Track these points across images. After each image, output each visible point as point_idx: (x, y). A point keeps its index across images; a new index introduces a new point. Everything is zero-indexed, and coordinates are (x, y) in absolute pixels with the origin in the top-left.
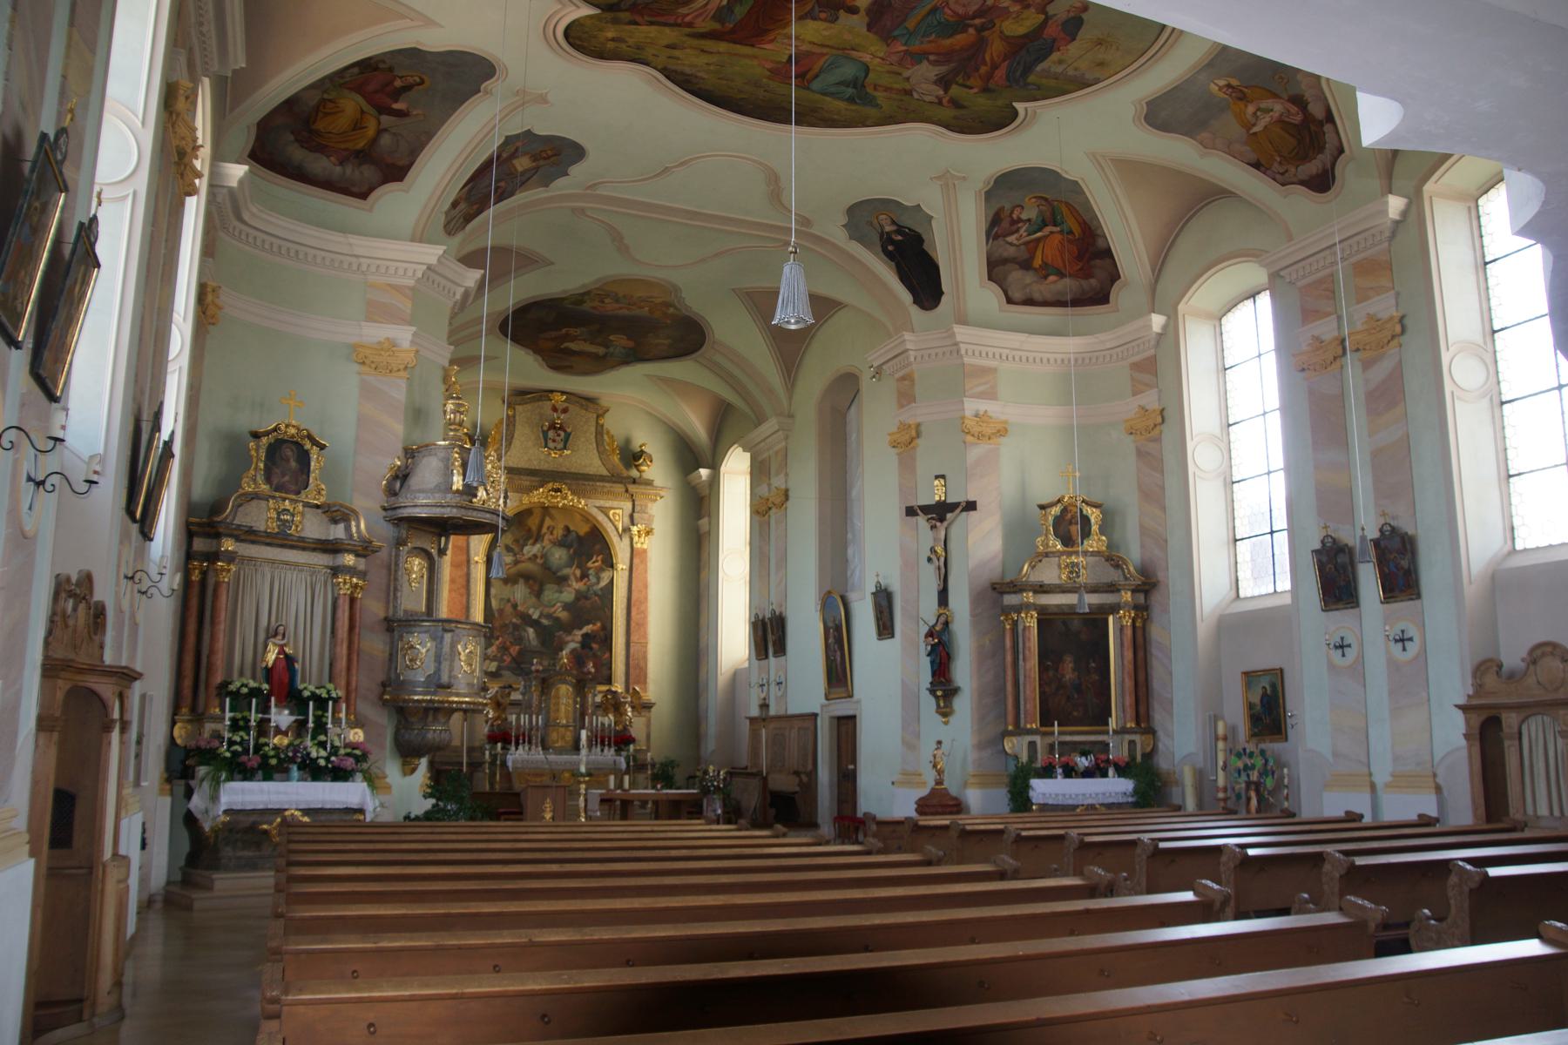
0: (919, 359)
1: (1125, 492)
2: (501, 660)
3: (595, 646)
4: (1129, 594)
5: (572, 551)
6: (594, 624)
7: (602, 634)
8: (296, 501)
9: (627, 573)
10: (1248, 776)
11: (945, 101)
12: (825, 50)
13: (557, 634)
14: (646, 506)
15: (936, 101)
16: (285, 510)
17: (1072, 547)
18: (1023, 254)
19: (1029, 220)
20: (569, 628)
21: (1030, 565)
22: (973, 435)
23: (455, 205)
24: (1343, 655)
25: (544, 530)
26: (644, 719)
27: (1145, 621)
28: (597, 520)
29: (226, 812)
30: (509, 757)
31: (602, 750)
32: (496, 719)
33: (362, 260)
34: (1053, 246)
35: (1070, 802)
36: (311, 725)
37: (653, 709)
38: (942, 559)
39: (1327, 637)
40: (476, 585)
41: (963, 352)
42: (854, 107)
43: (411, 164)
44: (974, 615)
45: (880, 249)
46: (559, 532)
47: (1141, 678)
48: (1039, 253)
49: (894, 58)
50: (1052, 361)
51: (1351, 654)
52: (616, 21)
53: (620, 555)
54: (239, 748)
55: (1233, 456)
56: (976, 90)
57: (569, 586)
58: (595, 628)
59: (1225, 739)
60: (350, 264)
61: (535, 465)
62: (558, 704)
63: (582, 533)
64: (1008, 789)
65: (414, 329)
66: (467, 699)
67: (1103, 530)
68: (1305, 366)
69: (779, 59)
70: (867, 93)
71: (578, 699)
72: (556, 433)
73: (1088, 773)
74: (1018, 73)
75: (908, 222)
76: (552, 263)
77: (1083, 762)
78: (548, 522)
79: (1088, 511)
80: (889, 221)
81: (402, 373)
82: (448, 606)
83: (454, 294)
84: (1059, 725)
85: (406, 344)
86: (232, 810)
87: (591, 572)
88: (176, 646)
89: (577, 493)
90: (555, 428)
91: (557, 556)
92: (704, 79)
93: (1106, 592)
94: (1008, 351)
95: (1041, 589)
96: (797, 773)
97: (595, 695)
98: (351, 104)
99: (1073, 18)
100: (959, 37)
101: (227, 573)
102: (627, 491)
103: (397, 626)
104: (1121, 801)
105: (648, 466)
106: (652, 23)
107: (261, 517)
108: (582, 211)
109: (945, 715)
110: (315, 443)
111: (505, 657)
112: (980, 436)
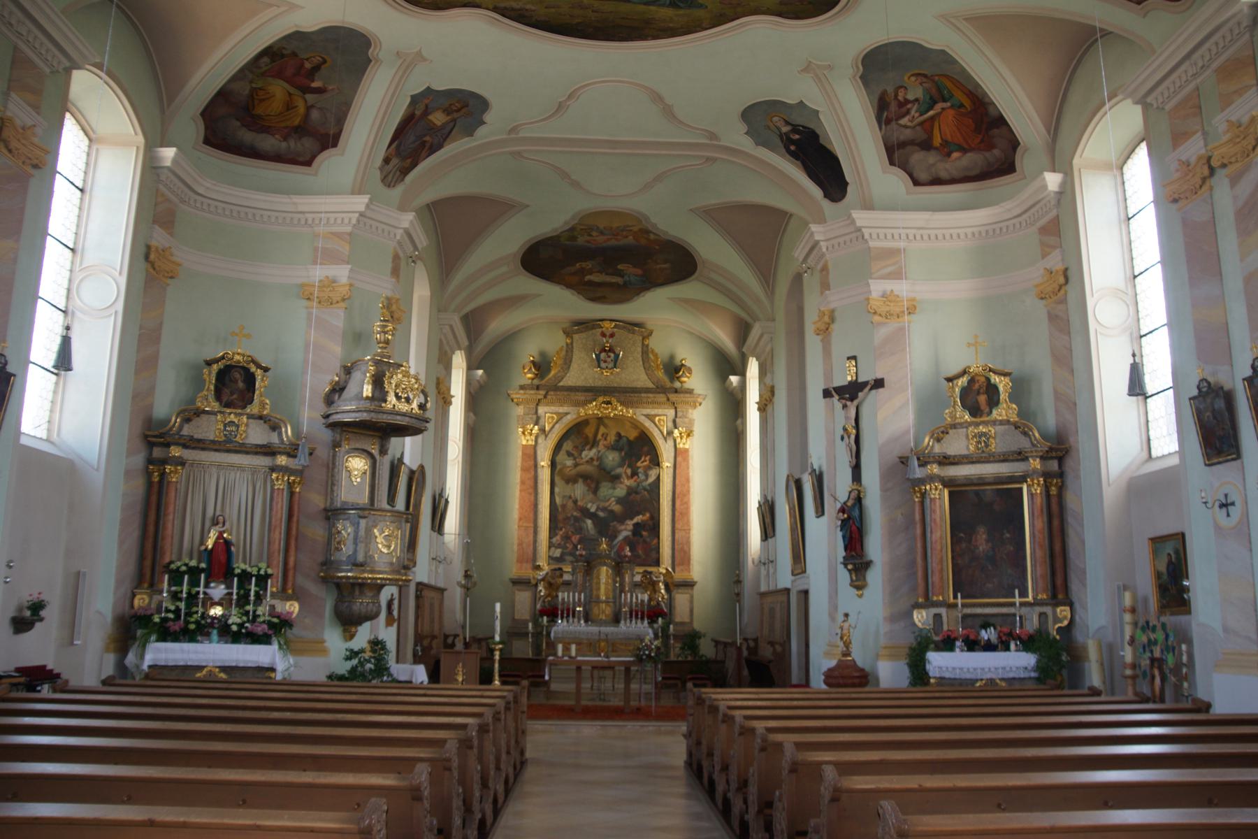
0: (830, 249)
1: (1038, 360)
2: (564, 547)
3: (644, 533)
4: (1038, 460)
5: (623, 454)
6: (644, 515)
7: (650, 523)
8: (241, 414)
9: (672, 470)
10: (1152, 652)
13: (612, 524)
14: (687, 412)
16: (230, 422)
17: (981, 416)
18: (920, 134)
19: (917, 100)
20: (622, 519)
21: (931, 437)
22: (880, 315)
23: (387, 161)
24: (1228, 515)
25: (599, 437)
26: (688, 595)
27: (1061, 488)
28: (645, 427)
29: (150, 667)
30: (554, 629)
31: (636, 623)
32: (546, 596)
33: (307, 215)
34: (948, 125)
35: (968, 676)
36: (252, 598)
37: (695, 588)
38: (853, 437)
39: (1203, 495)
40: (542, 485)
41: (867, 236)
42: (681, 12)
43: (341, 131)
44: (884, 489)
45: (784, 150)
46: (612, 438)
47: (1057, 547)
48: (936, 132)
50: (962, 236)
51: (1235, 512)
54: (171, 616)
55: (1140, 309)
57: (621, 483)
58: (645, 518)
59: (1133, 610)
60: (299, 220)
61: (590, 383)
62: (599, 583)
63: (631, 438)
64: (907, 661)
65: (350, 266)
66: (389, 577)
67: (1015, 397)
68: (1176, 196)
71: (618, 579)
72: (607, 355)
73: (989, 647)
75: (799, 120)
76: (528, 206)
77: (987, 635)
78: (602, 430)
79: (995, 379)
80: (783, 123)
81: (342, 305)
82: (520, 504)
83: (395, 235)
84: (962, 598)
85: (344, 280)
86: (156, 665)
87: (640, 470)
88: (135, 534)
89: (626, 404)
90: (605, 351)
91: (611, 458)
92: (534, 11)
93: (1018, 460)
94: (914, 231)
95: (945, 461)
96: (772, 644)
97: (633, 575)
98: (278, 89)
101: (176, 476)
102: (668, 400)
103: (332, 514)
104: (1022, 676)
105: (689, 378)
107: (209, 429)
108: (519, 153)
109: (859, 588)
110: (259, 366)
111: (568, 545)
112: (888, 315)
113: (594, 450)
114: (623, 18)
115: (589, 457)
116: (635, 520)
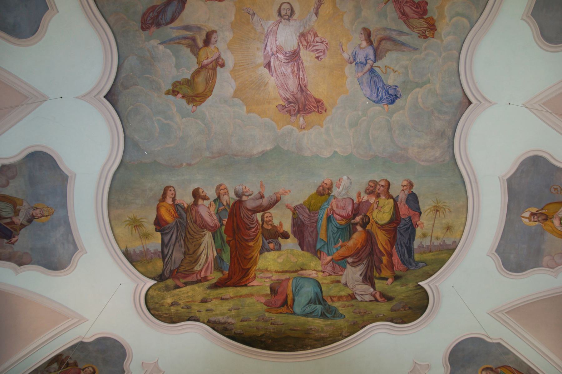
11: (378, 296)
12: (287, 276)
15: (373, 299)
42: (329, 322)
49: (329, 269)
52: (167, 289)
56: (390, 280)
69: (265, 293)
70: (329, 305)
74: (406, 255)
92: (233, 324)
99: (409, 194)
100: (355, 236)
106: (186, 284)
114: (291, 330)
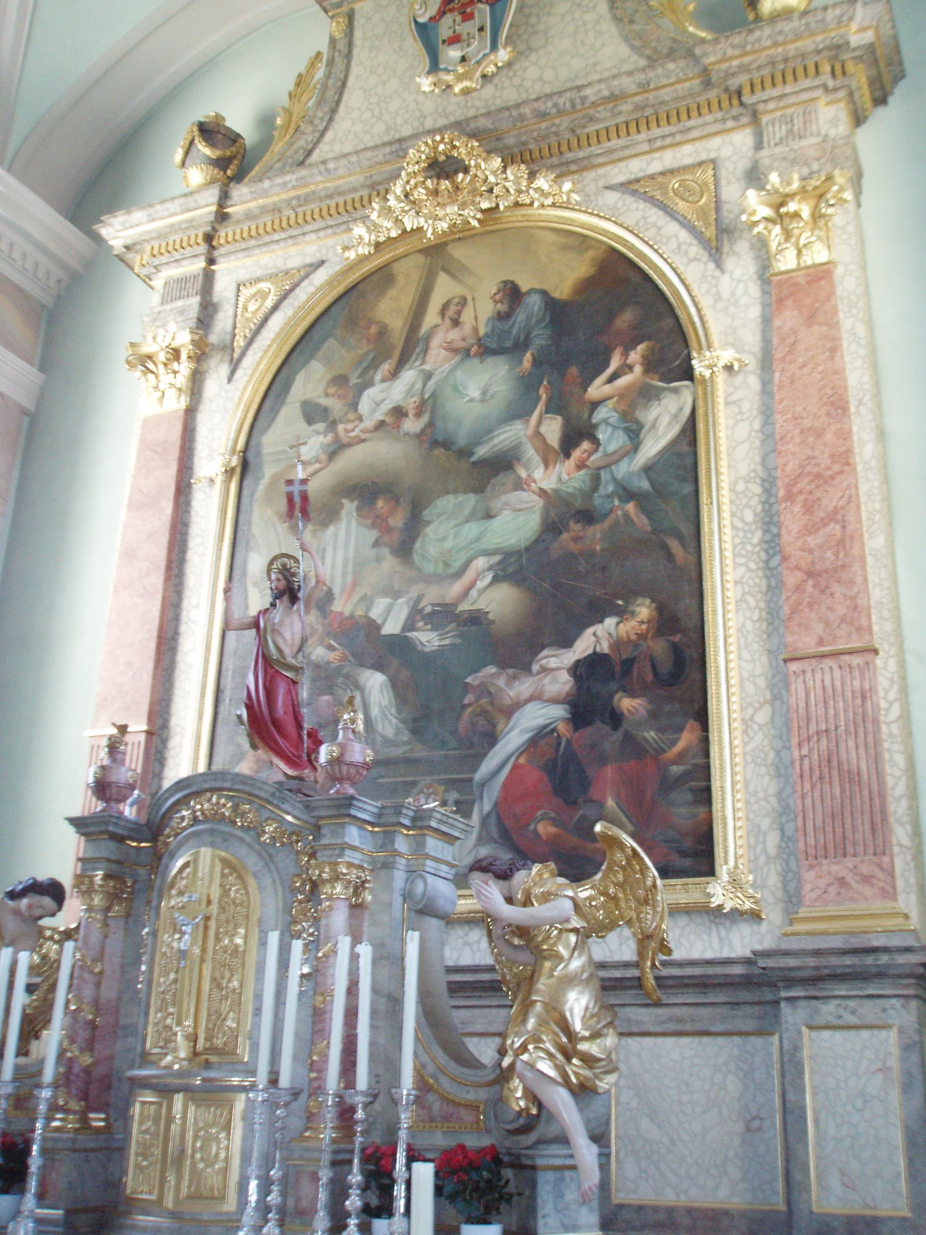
3: (627, 704)
5: (528, 356)
6: (622, 614)
7: (659, 647)
25: (431, 318)
53: (716, 326)
57: (519, 485)
58: (629, 628)
63: (562, 290)
87: (601, 414)
91: (475, 393)
113: (409, 375)
115: (387, 406)
116: (584, 645)
